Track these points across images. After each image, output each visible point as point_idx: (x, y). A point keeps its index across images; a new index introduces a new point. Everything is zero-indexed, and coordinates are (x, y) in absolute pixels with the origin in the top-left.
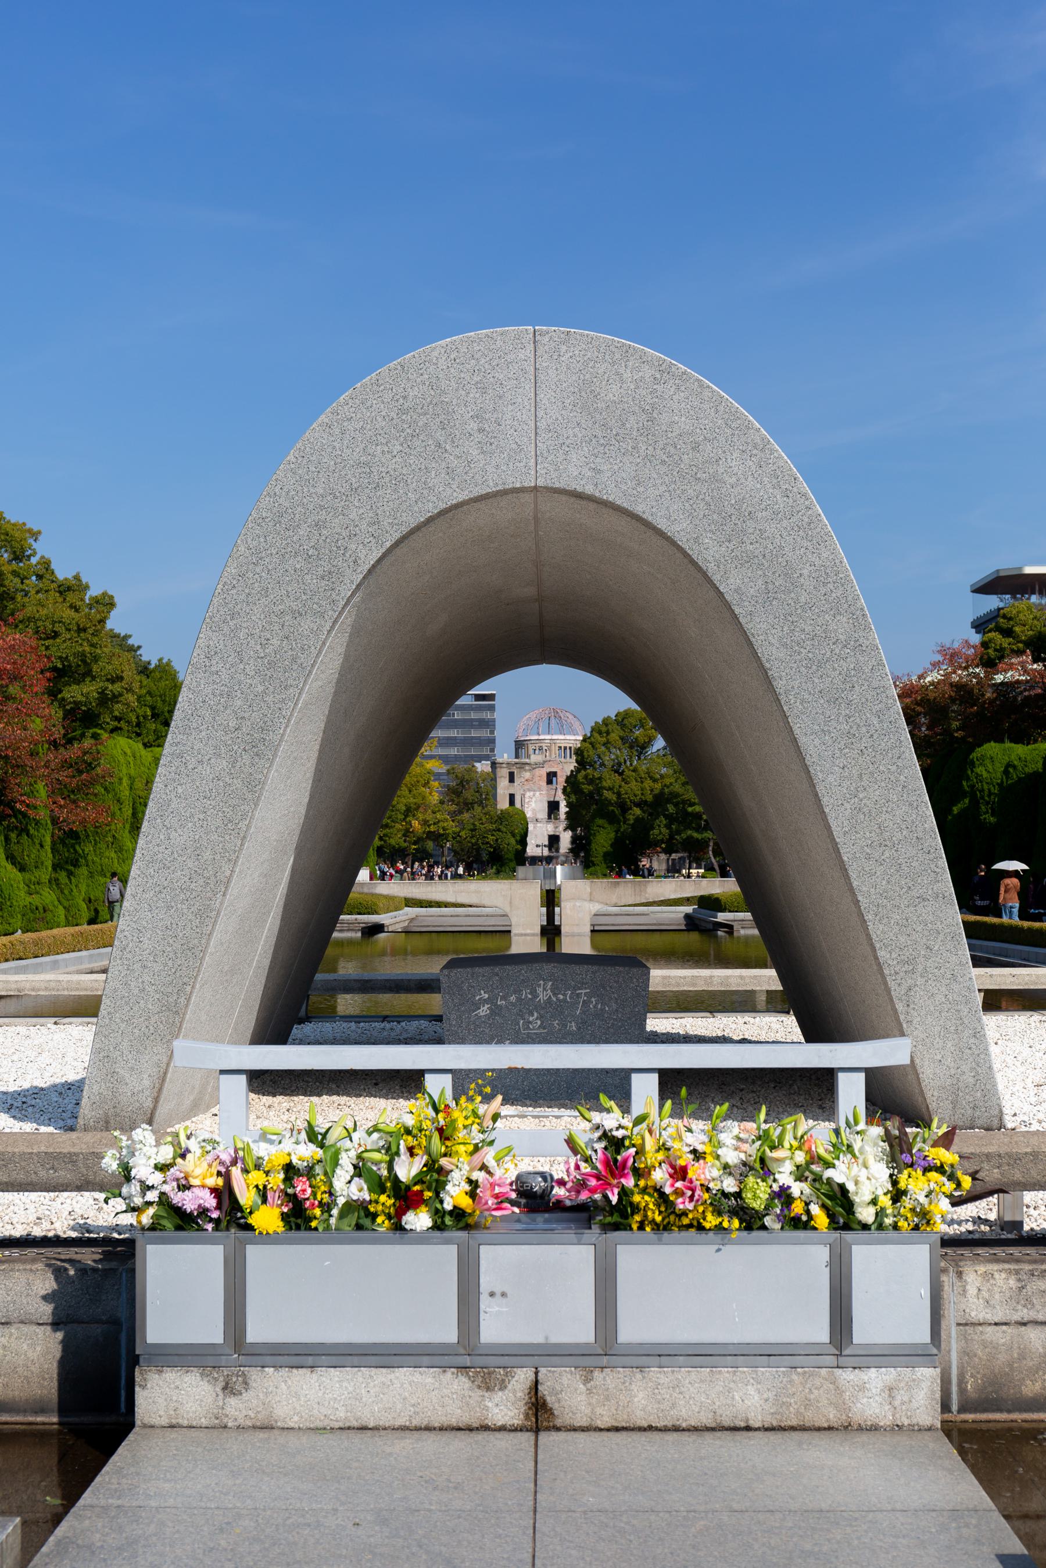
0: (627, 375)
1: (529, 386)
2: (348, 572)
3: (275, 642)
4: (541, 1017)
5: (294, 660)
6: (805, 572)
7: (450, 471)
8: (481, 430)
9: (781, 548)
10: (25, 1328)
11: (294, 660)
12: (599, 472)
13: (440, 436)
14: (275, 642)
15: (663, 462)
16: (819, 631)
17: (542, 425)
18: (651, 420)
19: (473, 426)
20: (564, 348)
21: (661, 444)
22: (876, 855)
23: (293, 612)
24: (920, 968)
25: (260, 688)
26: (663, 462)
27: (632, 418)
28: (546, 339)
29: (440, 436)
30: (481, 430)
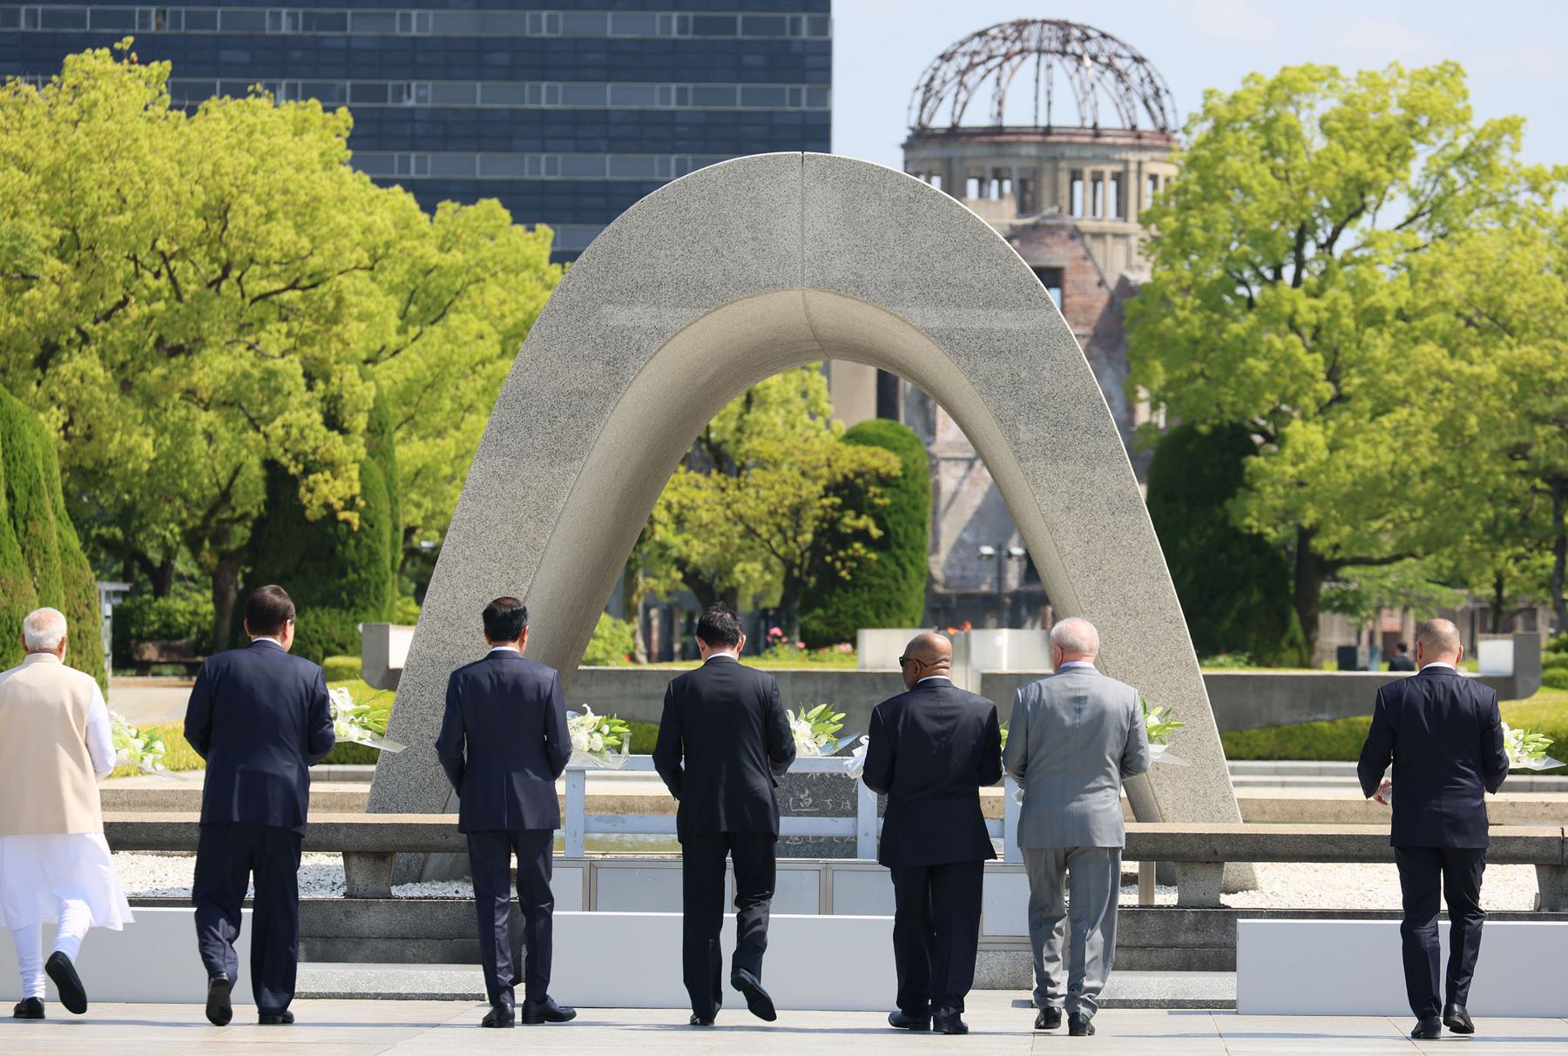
2: (632, 358)
4: (812, 795)
5: (579, 436)
6: (1048, 366)
9: (1026, 344)
10: (429, 942)
11: (579, 436)
13: (718, 242)
14: (563, 419)
15: (918, 269)
16: (1061, 418)
20: (829, 171)
23: (580, 393)
26: (918, 269)
27: (889, 232)
28: (813, 163)
29: (718, 242)
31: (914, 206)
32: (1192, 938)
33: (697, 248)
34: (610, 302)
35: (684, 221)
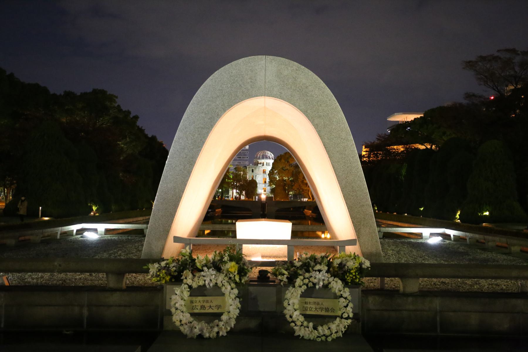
0: (289, 68)
1: (264, 71)
3: (196, 135)
7: (243, 92)
8: (251, 82)
11: (201, 140)
12: (281, 93)
14: (196, 135)
17: (267, 81)
18: (296, 80)
19: (249, 81)
21: (298, 86)
22: (351, 194)
24: (362, 223)
25: (192, 147)
29: (241, 83)
30: (251, 82)
31: (298, 72)
32: (411, 307)
33: (234, 85)
34: (209, 101)
35: (231, 76)
